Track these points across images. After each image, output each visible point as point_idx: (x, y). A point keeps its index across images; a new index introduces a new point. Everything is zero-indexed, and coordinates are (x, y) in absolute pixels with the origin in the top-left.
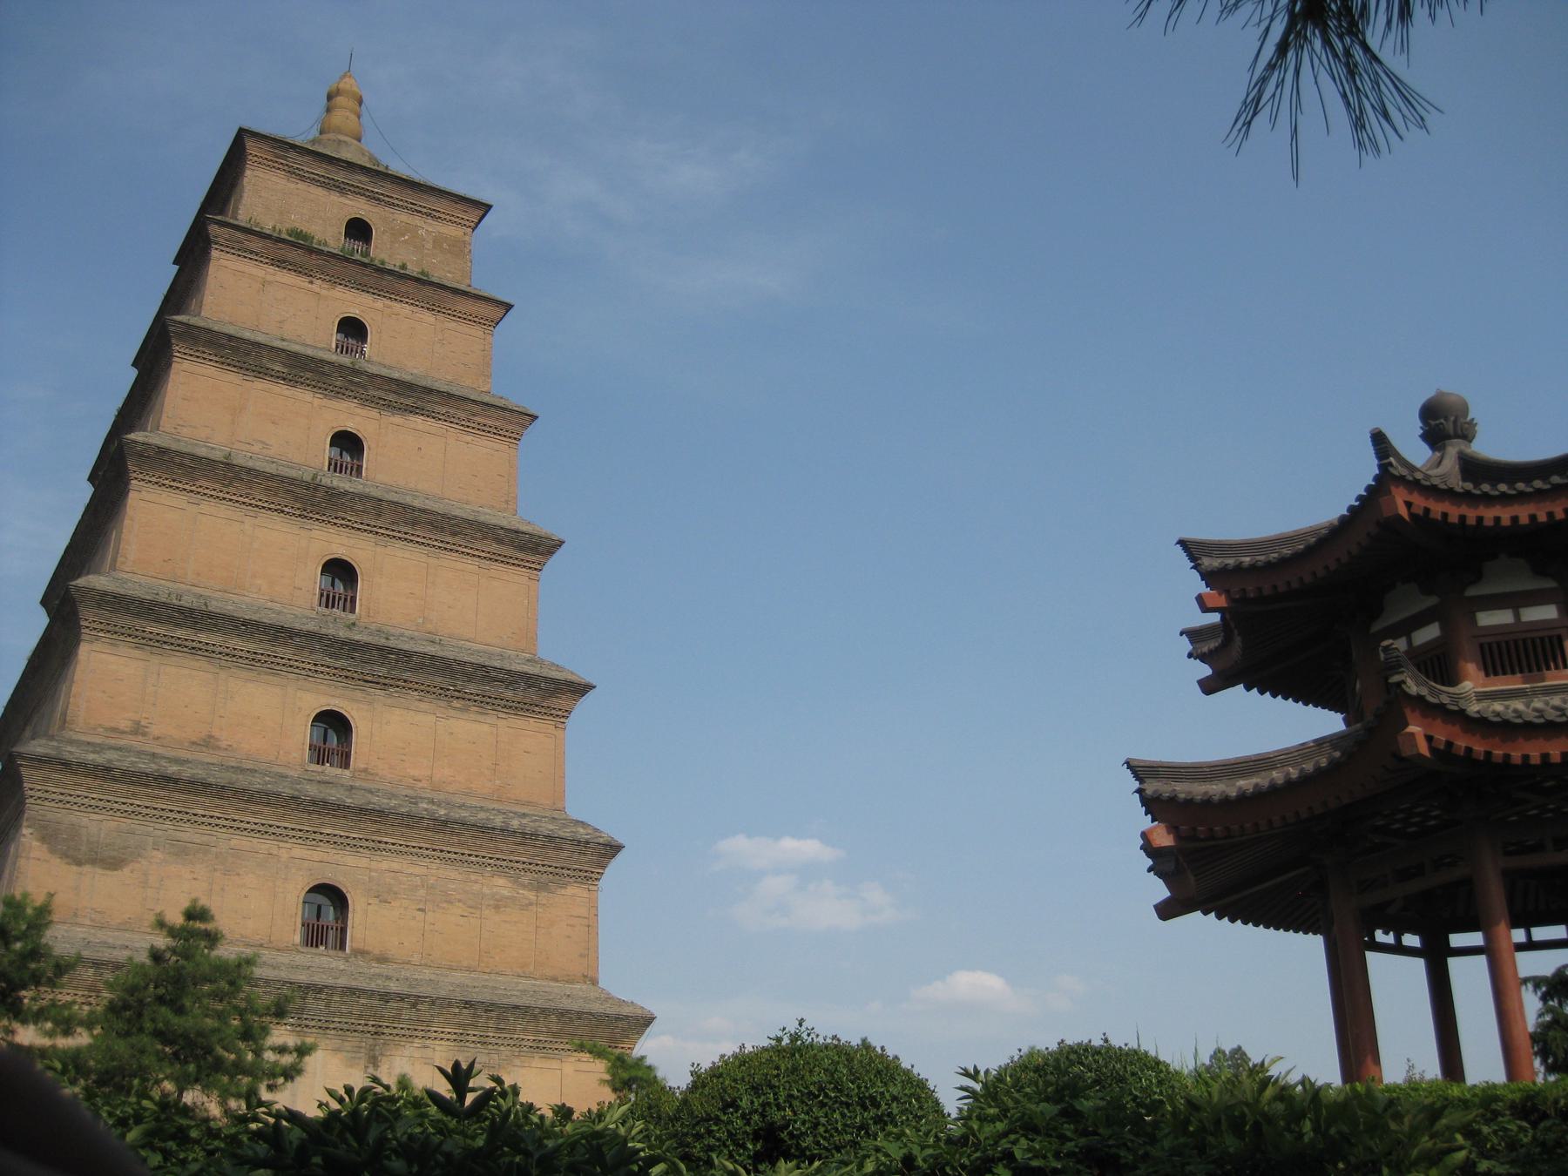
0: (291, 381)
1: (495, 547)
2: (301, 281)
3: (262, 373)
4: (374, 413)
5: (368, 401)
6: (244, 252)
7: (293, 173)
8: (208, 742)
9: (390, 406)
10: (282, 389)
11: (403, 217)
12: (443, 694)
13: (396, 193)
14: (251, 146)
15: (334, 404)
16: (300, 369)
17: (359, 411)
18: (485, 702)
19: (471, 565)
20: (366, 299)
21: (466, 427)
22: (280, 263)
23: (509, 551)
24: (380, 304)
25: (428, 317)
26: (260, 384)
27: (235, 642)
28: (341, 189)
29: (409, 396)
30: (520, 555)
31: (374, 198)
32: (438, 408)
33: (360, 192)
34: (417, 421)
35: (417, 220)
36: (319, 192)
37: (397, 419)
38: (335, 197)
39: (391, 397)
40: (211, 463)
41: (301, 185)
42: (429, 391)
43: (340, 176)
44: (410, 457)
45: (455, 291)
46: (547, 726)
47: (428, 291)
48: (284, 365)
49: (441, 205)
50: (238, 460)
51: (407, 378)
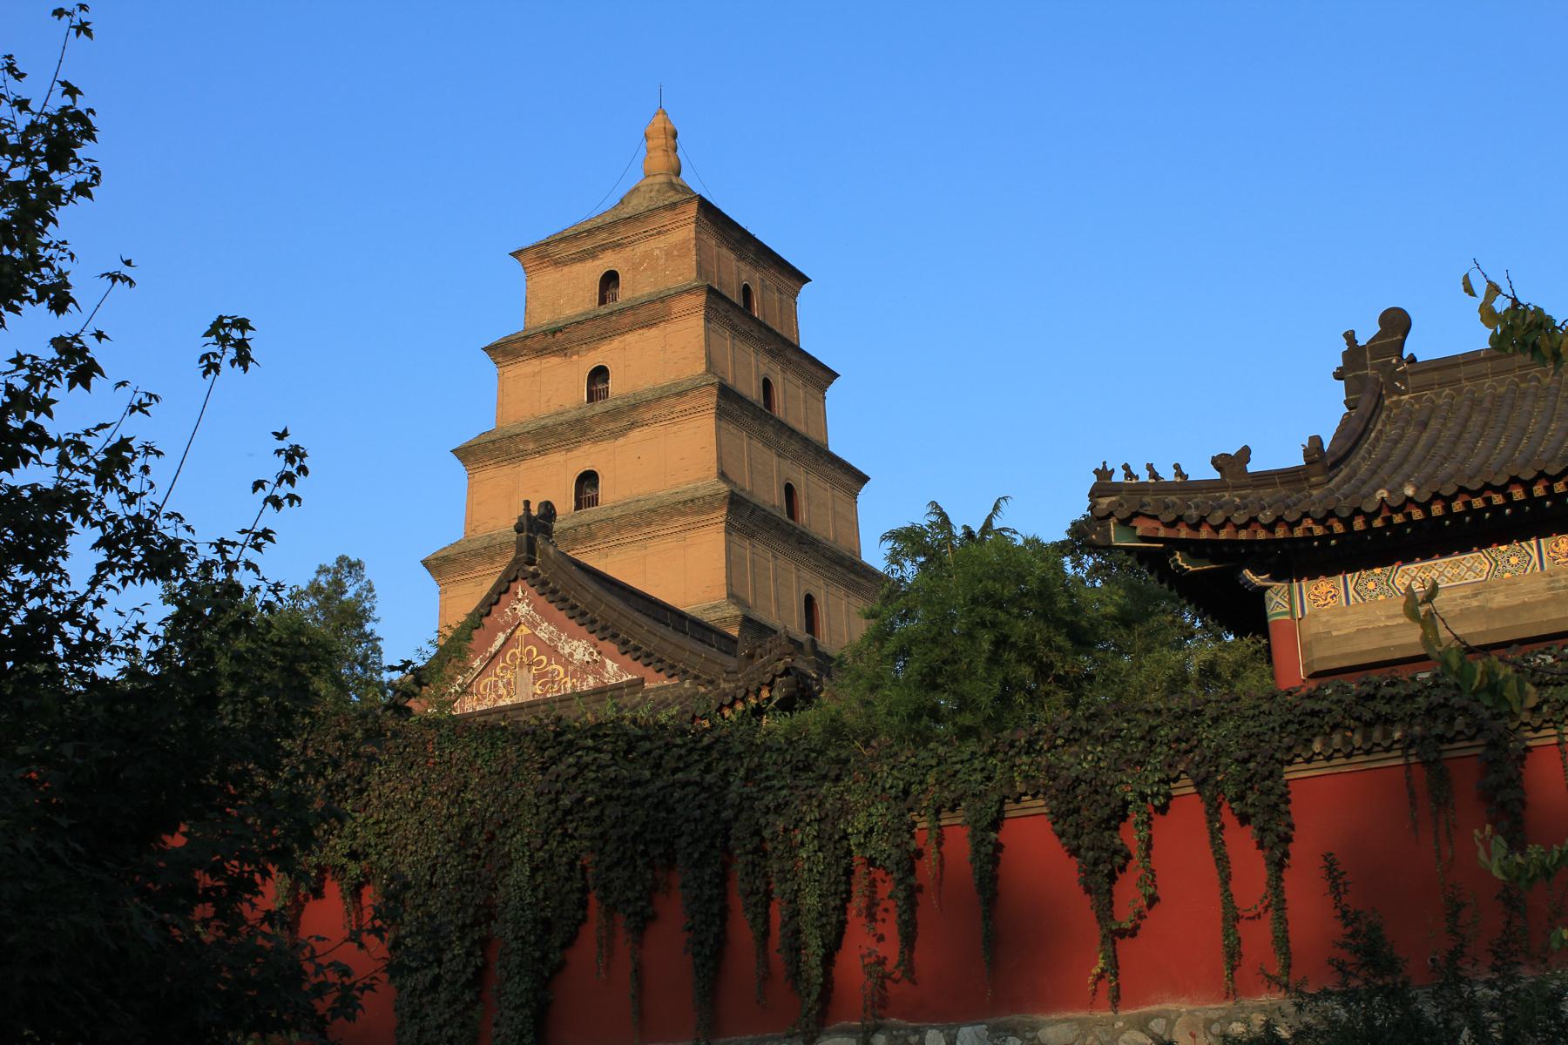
0: (542, 451)
1: (682, 520)
3: (523, 455)
4: (604, 445)
7: (558, 263)
10: (539, 461)
11: (641, 248)
15: (575, 453)
17: (595, 448)
23: (696, 519)
24: (616, 343)
25: (654, 332)
26: (524, 465)
28: (592, 254)
30: (704, 517)
31: (617, 246)
32: (646, 416)
33: (604, 248)
34: (635, 434)
37: (621, 441)
38: (589, 264)
39: (611, 426)
41: (566, 269)
42: (635, 407)
43: (588, 245)
47: (643, 314)
48: (536, 441)
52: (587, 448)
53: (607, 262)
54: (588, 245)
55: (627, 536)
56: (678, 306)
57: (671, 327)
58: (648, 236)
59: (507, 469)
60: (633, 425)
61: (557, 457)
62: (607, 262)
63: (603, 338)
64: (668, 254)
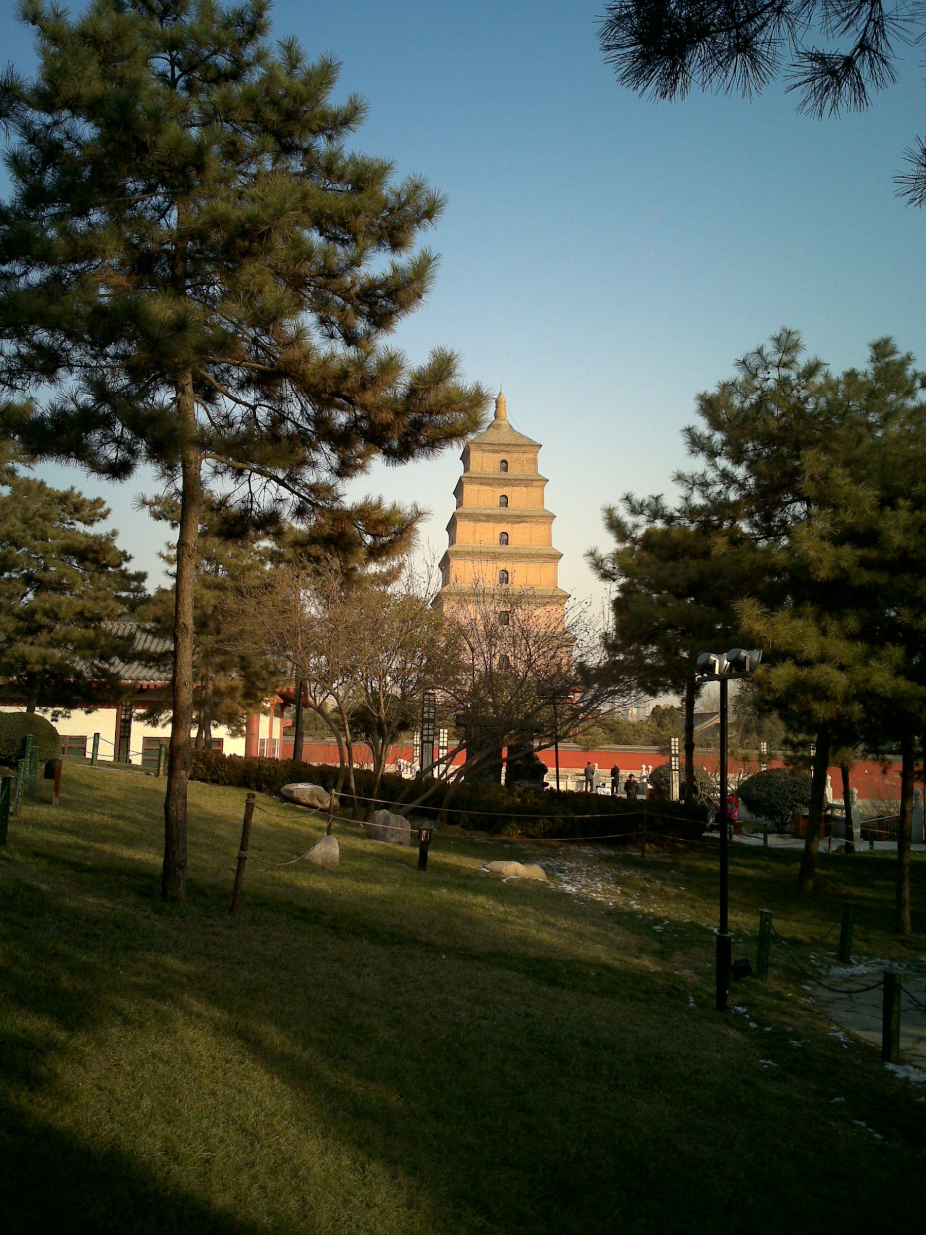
2: (488, 488)
3: (481, 521)
5: (508, 522)
6: (472, 483)
7: (483, 450)
9: (515, 523)
10: (486, 524)
11: (516, 455)
13: (514, 449)
14: (471, 446)
16: (489, 518)
19: (538, 565)
20: (506, 488)
21: (537, 522)
22: (482, 484)
25: (525, 489)
26: (480, 524)
28: (497, 452)
29: (519, 519)
31: (507, 452)
35: (521, 455)
36: (491, 454)
40: (469, 552)
43: (496, 448)
44: (520, 535)
45: (532, 480)
50: (475, 550)
53: (504, 456)
54: (496, 448)
55: (524, 559)
56: (535, 483)
58: (519, 452)
59: (472, 524)
61: (491, 524)
62: (504, 456)
64: (527, 462)
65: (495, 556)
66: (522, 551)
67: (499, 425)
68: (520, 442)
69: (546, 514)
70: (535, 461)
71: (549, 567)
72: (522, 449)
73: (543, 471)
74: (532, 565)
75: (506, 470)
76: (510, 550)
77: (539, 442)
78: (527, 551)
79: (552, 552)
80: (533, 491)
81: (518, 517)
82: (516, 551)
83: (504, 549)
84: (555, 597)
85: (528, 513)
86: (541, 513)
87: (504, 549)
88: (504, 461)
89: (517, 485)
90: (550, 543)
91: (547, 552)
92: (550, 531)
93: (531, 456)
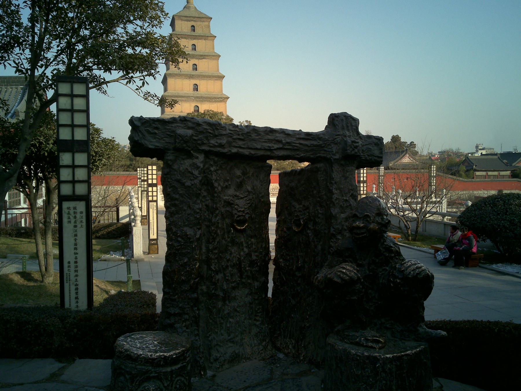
2: (185, 40)
5: (197, 59)
7: (182, 20)
8: (182, 112)
11: (199, 23)
12: (210, 101)
14: (175, 17)
18: (215, 102)
19: (213, 81)
20: (194, 40)
25: (204, 41)
27: (183, 99)
29: (202, 57)
31: (195, 21)
33: (192, 21)
35: (201, 23)
36: (186, 22)
43: (189, 19)
46: (224, 103)
49: (205, 20)
51: (201, 54)
52: (195, 59)
53: (193, 23)
54: (189, 19)
57: (207, 41)
60: (203, 58)
62: (193, 23)
63: (194, 39)
65: (190, 77)
66: (204, 74)
67: (189, 7)
68: (201, 16)
69: (216, 54)
70: (209, 27)
71: (218, 82)
72: (202, 20)
73: (213, 32)
74: (210, 81)
75: (194, 31)
76: (198, 74)
77: (210, 16)
78: (207, 74)
79: (219, 75)
80: (208, 42)
81: (202, 56)
82: (201, 74)
83: (195, 73)
84: (221, 98)
85: (206, 54)
86: (213, 54)
87: (195, 73)
88: (193, 26)
89: (200, 39)
90: (218, 70)
91: (217, 75)
92: (218, 64)
93: (207, 23)
